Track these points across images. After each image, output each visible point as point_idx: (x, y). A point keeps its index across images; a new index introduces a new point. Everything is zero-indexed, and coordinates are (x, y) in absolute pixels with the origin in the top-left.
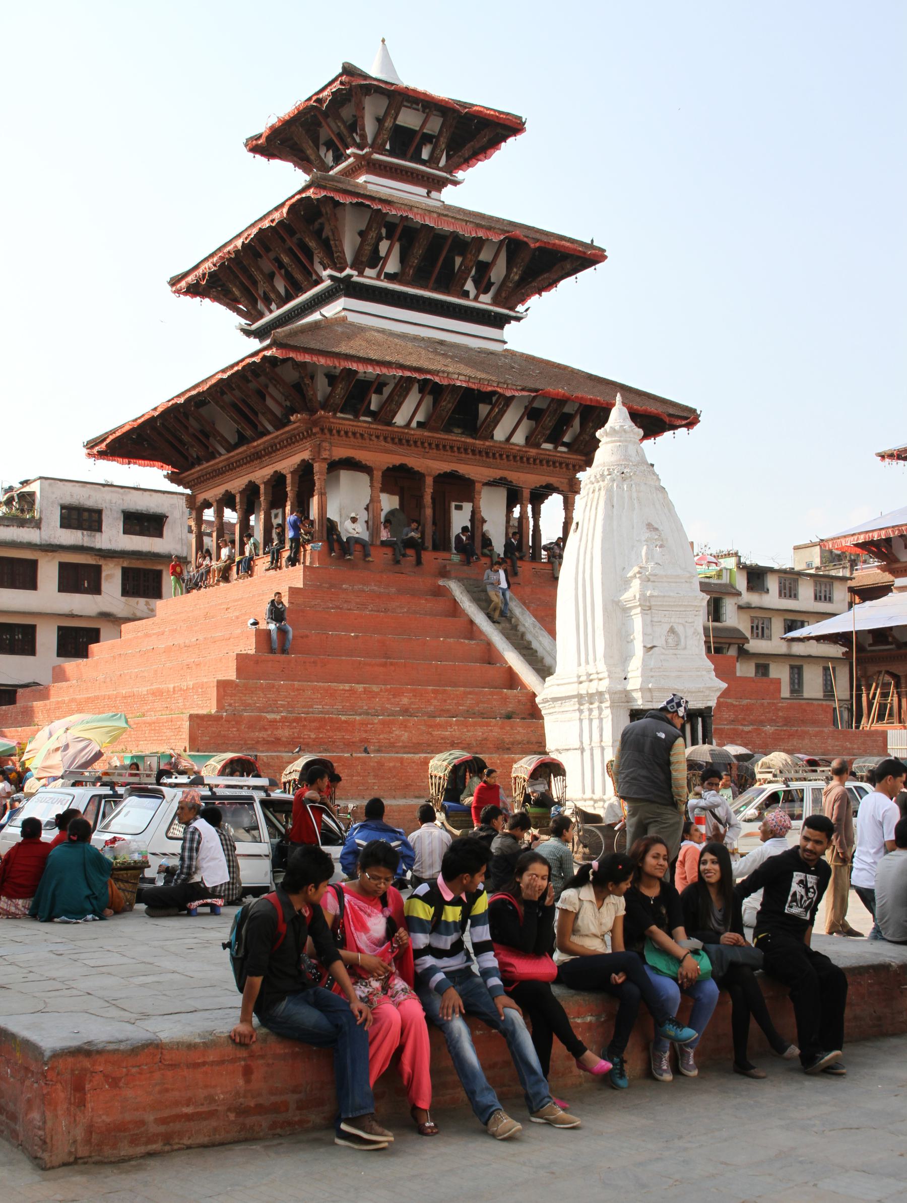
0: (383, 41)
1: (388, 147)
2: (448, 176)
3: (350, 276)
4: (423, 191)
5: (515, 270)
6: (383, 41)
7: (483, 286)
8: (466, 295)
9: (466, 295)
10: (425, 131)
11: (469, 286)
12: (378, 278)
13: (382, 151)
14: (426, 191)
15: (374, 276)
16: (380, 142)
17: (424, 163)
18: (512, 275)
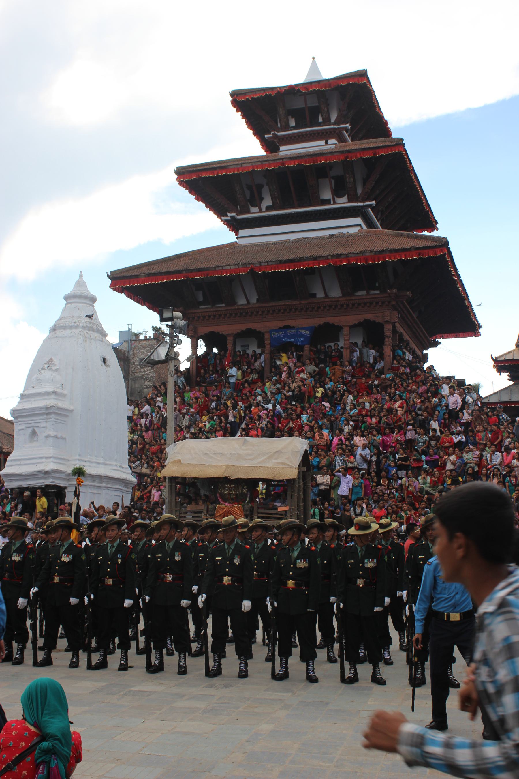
0: (314, 58)
1: (293, 123)
2: (335, 126)
3: (232, 217)
4: (323, 142)
5: (347, 175)
6: (314, 58)
7: (337, 193)
8: (328, 202)
9: (328, 202)
10: (309, 105)
11: (327, 195)
12: (261, 211)
13: (287, 127)
14: (324, 141)
15: (258, 211)
16: (284, 124)
17: (320, 124)
18: (347, 179)
